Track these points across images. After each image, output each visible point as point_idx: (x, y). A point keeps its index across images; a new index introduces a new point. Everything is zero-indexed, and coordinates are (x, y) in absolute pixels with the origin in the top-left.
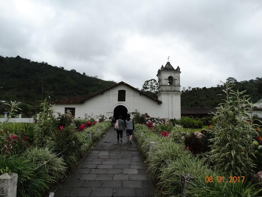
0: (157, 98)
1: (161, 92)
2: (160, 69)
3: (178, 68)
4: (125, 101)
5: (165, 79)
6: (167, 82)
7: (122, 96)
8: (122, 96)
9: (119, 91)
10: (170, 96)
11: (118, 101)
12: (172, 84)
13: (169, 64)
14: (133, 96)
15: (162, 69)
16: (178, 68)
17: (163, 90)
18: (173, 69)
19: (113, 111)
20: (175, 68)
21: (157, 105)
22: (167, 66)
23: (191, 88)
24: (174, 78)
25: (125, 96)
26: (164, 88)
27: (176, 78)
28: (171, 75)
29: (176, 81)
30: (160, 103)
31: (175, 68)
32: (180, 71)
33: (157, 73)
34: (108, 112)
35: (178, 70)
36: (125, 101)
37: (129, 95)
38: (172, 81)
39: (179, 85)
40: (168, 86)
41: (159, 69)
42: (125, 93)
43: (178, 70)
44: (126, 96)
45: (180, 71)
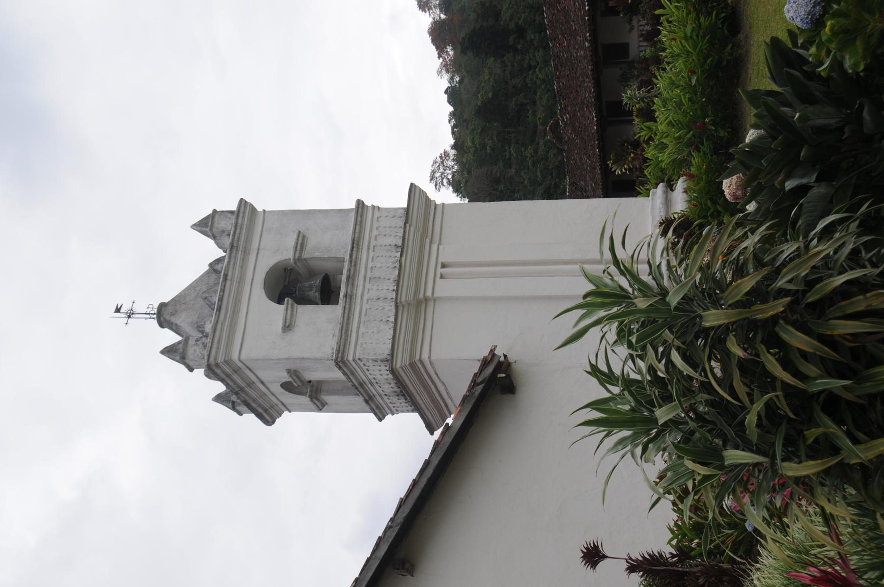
2: (219, 387)
3: (207, 226)
5: (288, 327)
6: (318, 324)
10: (443, 289)
13: (170, 309)
16: (207, 226)
17: (385, 349)
20: (209, 251)
24: (287, 254)
26: (373, 341)
27: (291, 241)
28: (260, 277)
29: (312, 242)
31: (209, 251)
32: (234, 207)
33: (250, 418)
35: (226, 224)
39: (353, 215)
43: (234, 228)
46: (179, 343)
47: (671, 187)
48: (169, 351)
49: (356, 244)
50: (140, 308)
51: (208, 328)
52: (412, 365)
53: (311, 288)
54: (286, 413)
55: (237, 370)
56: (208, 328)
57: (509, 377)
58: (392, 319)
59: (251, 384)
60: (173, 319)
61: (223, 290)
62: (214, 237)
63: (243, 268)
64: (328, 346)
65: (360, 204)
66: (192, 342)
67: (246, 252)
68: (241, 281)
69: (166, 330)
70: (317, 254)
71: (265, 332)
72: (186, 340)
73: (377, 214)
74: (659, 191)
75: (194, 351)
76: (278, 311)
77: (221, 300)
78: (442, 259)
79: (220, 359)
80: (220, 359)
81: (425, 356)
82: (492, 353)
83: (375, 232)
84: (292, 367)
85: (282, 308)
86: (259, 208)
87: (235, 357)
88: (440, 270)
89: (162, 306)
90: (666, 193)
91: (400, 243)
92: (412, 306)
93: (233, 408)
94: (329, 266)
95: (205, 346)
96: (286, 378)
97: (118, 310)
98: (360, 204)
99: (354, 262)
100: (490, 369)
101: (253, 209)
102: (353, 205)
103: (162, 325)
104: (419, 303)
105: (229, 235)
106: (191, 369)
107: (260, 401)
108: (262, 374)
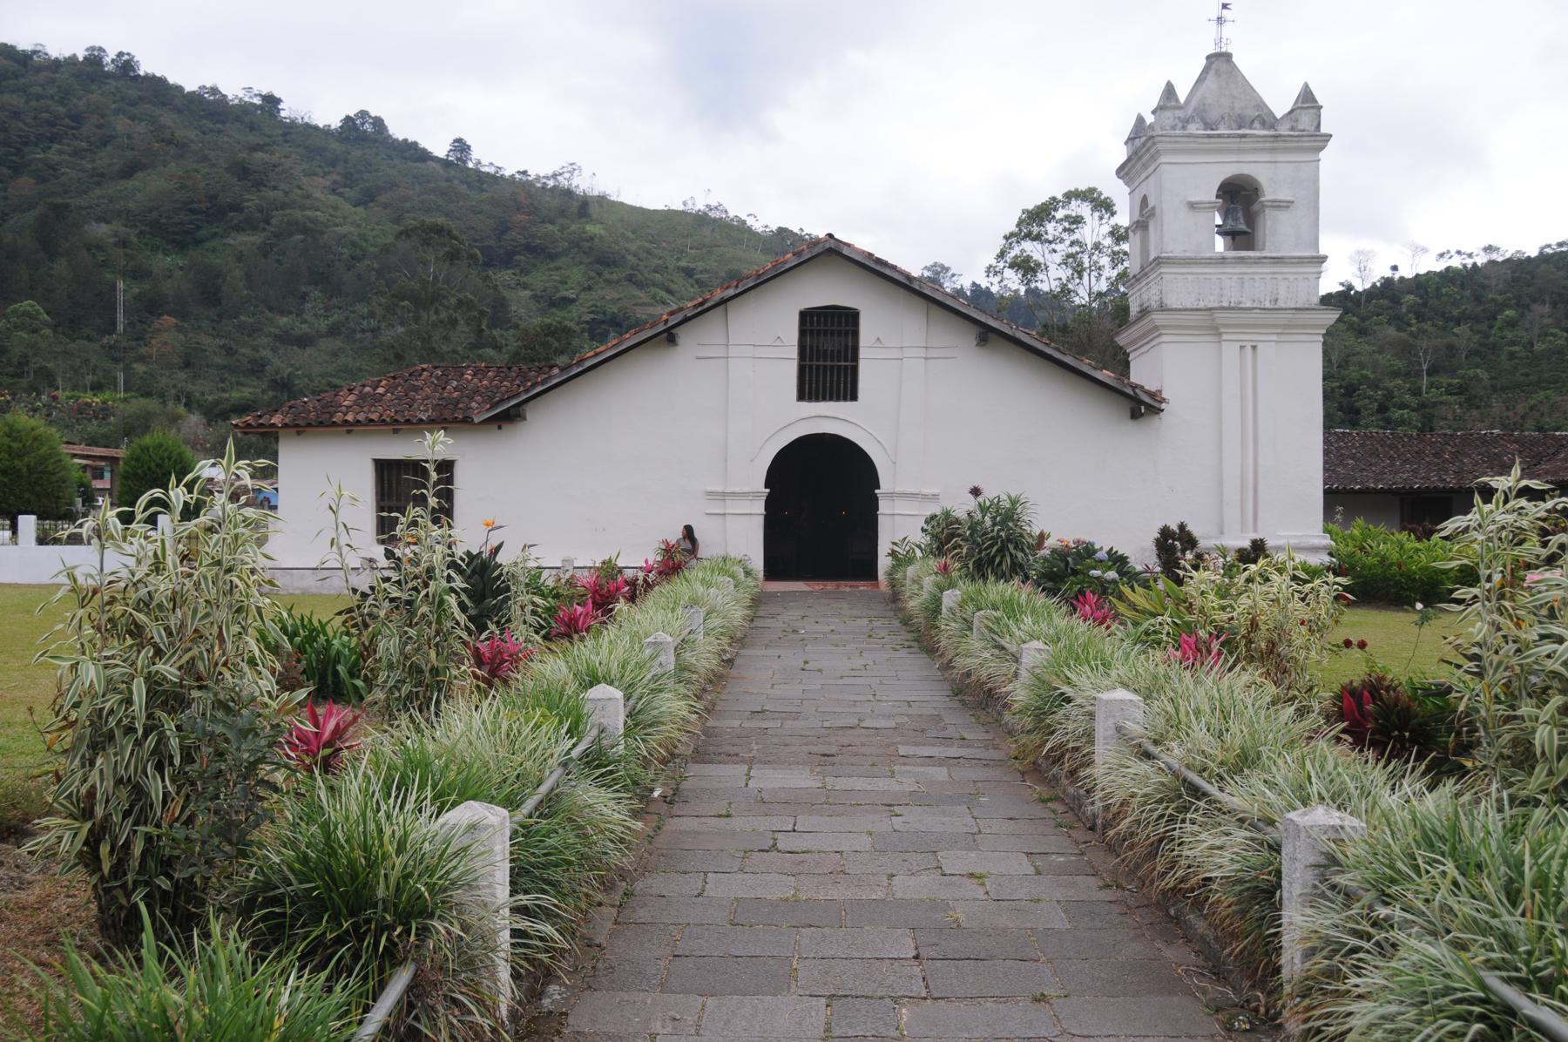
0: (1124, 366)
1: (1158, 318)
3: (1307, 99)
4: (854, 397)
5: (1193, 206)
7: (828, 356)
8: (828, 356)
9: (806, 316)
10: (1230, 350)
11: (802, 396)
12: (1251, 247)
13: (1224, 66)
14: (922, 353)
15: (1168, 114)
16: (1307, 99)
17: (1173, 302)
18: (1267, 120)
19: (756, 480)
20: (1280, 102)
21: (1132, 426)
22: (1211, 81)
23: (1425, 250)
24: (1269, 194)
25: (855, 358)
26: (1178, 289)
27: (1283, 195)
28: (1245, 170)
29: (1282, 215)
30: (1141, 406)
31: (1280, 102)
32: (1323, 130)
33: (1122, 156)
34: (720, 489)
35: (1305, 121)
36: (854, 397)
37: (887, 343)
38: (1251, 219)
40: (1222, 260)
41: (1140, 120)
42: (856, 334)
43: (1302, 130)
44: (862, 353)
45: (1323, 130)
46: (1177, 100)
47: (1331, 554)
48: (1169, 91)
49: (1278, 260)
50: (1226, 27)
51: (1193, 128)
52: (1156, 328)
53: (1236, 220)
54: (1128, 190)
55: (1154, 158)
56: (1193, 128)
57: (1142, 415)
58: (1201, 305)
59: (1145, 166)
60: (1212, 73)
61: (1229, 136)
62: (1291, 112)
63: (1255, 150)
64: (1175, 249)
65: (1324, 259)
66: (1178, 113)
67: (1273, 150)
68: (1240, 151)
69: (1204, 62)
70: (1269, 223)
71: (1194, 180)
72: (1180, 108)
73: (1312, 277)
74: (1327, 541)
75: (1169, 116)
76: (1209, 194)
77: (1219, 136)
78: (1260, 346)
79: (1159, 146)
80: (1159, 146)
81: (1164, 338)
82: (1163, 400)
83: (1291, 277)
84: (1158, 211)
85: (1213, 198)
86: (1322, 155)
87: (1163, 159)
88: (1249, 345)
89: (1227, 57)
90: (1325, 548)
91: (1281, 304)
92: (1212, 322)
93: (1129, 139)
94: (1259, 235)
95: (1174, 128)
96: (1151, 203)
97: (1225, 6)
98: (1324, 259)
99: (1258, 261)
100: (1147, 399)
101: (1322, 149)
102: (1322, 252)
103: (1208, 58)
104: (1216, 328)
105: (1292, 129)
106: (1154, 112)
107: (1139, 165)
108: (1151, 179)
